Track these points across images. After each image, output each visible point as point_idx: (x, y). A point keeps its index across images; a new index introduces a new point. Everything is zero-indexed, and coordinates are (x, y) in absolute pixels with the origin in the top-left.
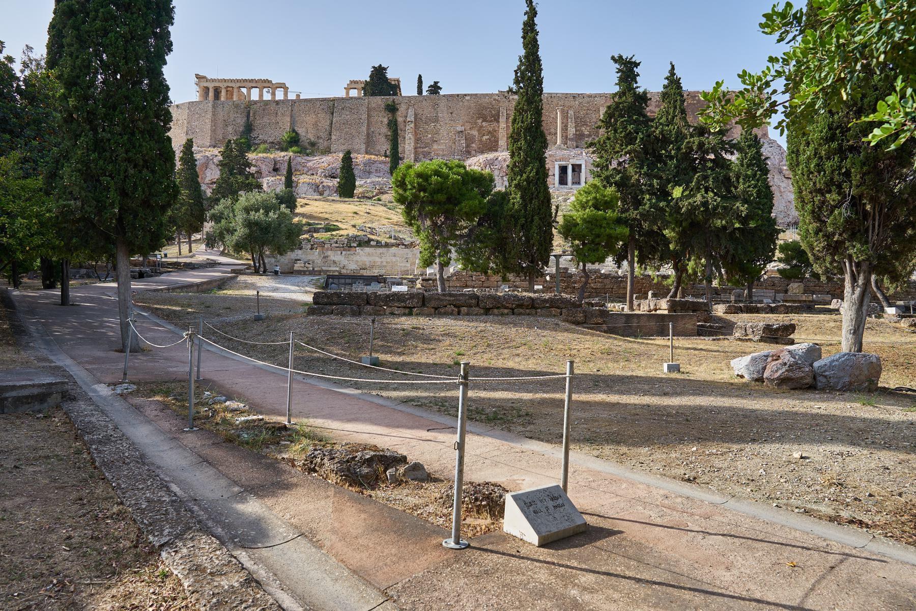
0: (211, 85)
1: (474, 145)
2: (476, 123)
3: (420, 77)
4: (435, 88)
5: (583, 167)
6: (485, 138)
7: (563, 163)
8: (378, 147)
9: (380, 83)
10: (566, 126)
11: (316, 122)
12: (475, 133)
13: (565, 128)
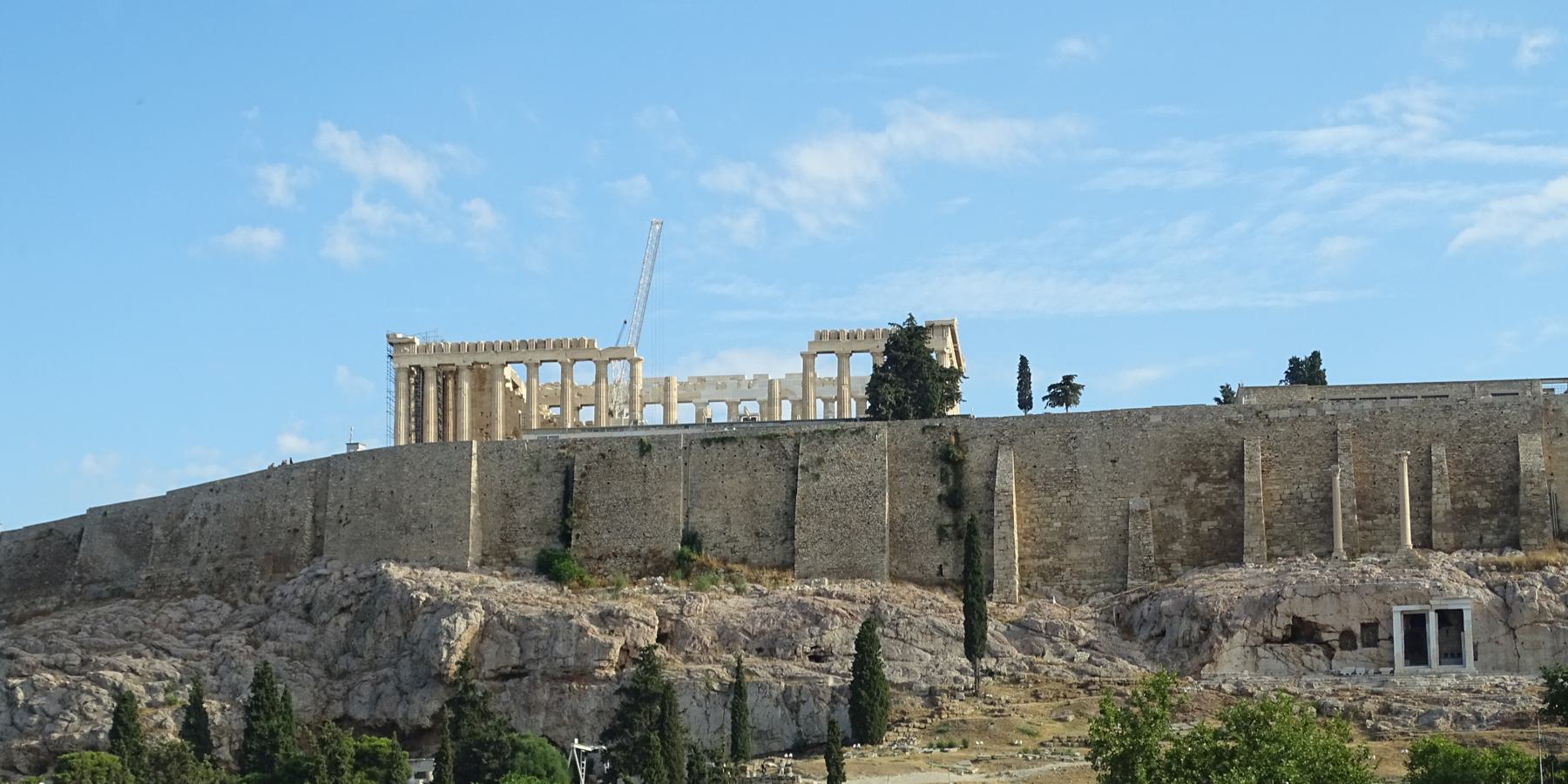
0: (428, 362)
1: (1177, 547)
2: (1178, 486)
3: (1024, 363)
4: (1065, 391)
5: (1467, 617)
6: (1206, 526)
7: (1414, 608)
8: (920, 558)
9: (910, 372)
10: (1427, 488)
11: (751, 494)
12: (1179, 513)
13: (1423, 495)
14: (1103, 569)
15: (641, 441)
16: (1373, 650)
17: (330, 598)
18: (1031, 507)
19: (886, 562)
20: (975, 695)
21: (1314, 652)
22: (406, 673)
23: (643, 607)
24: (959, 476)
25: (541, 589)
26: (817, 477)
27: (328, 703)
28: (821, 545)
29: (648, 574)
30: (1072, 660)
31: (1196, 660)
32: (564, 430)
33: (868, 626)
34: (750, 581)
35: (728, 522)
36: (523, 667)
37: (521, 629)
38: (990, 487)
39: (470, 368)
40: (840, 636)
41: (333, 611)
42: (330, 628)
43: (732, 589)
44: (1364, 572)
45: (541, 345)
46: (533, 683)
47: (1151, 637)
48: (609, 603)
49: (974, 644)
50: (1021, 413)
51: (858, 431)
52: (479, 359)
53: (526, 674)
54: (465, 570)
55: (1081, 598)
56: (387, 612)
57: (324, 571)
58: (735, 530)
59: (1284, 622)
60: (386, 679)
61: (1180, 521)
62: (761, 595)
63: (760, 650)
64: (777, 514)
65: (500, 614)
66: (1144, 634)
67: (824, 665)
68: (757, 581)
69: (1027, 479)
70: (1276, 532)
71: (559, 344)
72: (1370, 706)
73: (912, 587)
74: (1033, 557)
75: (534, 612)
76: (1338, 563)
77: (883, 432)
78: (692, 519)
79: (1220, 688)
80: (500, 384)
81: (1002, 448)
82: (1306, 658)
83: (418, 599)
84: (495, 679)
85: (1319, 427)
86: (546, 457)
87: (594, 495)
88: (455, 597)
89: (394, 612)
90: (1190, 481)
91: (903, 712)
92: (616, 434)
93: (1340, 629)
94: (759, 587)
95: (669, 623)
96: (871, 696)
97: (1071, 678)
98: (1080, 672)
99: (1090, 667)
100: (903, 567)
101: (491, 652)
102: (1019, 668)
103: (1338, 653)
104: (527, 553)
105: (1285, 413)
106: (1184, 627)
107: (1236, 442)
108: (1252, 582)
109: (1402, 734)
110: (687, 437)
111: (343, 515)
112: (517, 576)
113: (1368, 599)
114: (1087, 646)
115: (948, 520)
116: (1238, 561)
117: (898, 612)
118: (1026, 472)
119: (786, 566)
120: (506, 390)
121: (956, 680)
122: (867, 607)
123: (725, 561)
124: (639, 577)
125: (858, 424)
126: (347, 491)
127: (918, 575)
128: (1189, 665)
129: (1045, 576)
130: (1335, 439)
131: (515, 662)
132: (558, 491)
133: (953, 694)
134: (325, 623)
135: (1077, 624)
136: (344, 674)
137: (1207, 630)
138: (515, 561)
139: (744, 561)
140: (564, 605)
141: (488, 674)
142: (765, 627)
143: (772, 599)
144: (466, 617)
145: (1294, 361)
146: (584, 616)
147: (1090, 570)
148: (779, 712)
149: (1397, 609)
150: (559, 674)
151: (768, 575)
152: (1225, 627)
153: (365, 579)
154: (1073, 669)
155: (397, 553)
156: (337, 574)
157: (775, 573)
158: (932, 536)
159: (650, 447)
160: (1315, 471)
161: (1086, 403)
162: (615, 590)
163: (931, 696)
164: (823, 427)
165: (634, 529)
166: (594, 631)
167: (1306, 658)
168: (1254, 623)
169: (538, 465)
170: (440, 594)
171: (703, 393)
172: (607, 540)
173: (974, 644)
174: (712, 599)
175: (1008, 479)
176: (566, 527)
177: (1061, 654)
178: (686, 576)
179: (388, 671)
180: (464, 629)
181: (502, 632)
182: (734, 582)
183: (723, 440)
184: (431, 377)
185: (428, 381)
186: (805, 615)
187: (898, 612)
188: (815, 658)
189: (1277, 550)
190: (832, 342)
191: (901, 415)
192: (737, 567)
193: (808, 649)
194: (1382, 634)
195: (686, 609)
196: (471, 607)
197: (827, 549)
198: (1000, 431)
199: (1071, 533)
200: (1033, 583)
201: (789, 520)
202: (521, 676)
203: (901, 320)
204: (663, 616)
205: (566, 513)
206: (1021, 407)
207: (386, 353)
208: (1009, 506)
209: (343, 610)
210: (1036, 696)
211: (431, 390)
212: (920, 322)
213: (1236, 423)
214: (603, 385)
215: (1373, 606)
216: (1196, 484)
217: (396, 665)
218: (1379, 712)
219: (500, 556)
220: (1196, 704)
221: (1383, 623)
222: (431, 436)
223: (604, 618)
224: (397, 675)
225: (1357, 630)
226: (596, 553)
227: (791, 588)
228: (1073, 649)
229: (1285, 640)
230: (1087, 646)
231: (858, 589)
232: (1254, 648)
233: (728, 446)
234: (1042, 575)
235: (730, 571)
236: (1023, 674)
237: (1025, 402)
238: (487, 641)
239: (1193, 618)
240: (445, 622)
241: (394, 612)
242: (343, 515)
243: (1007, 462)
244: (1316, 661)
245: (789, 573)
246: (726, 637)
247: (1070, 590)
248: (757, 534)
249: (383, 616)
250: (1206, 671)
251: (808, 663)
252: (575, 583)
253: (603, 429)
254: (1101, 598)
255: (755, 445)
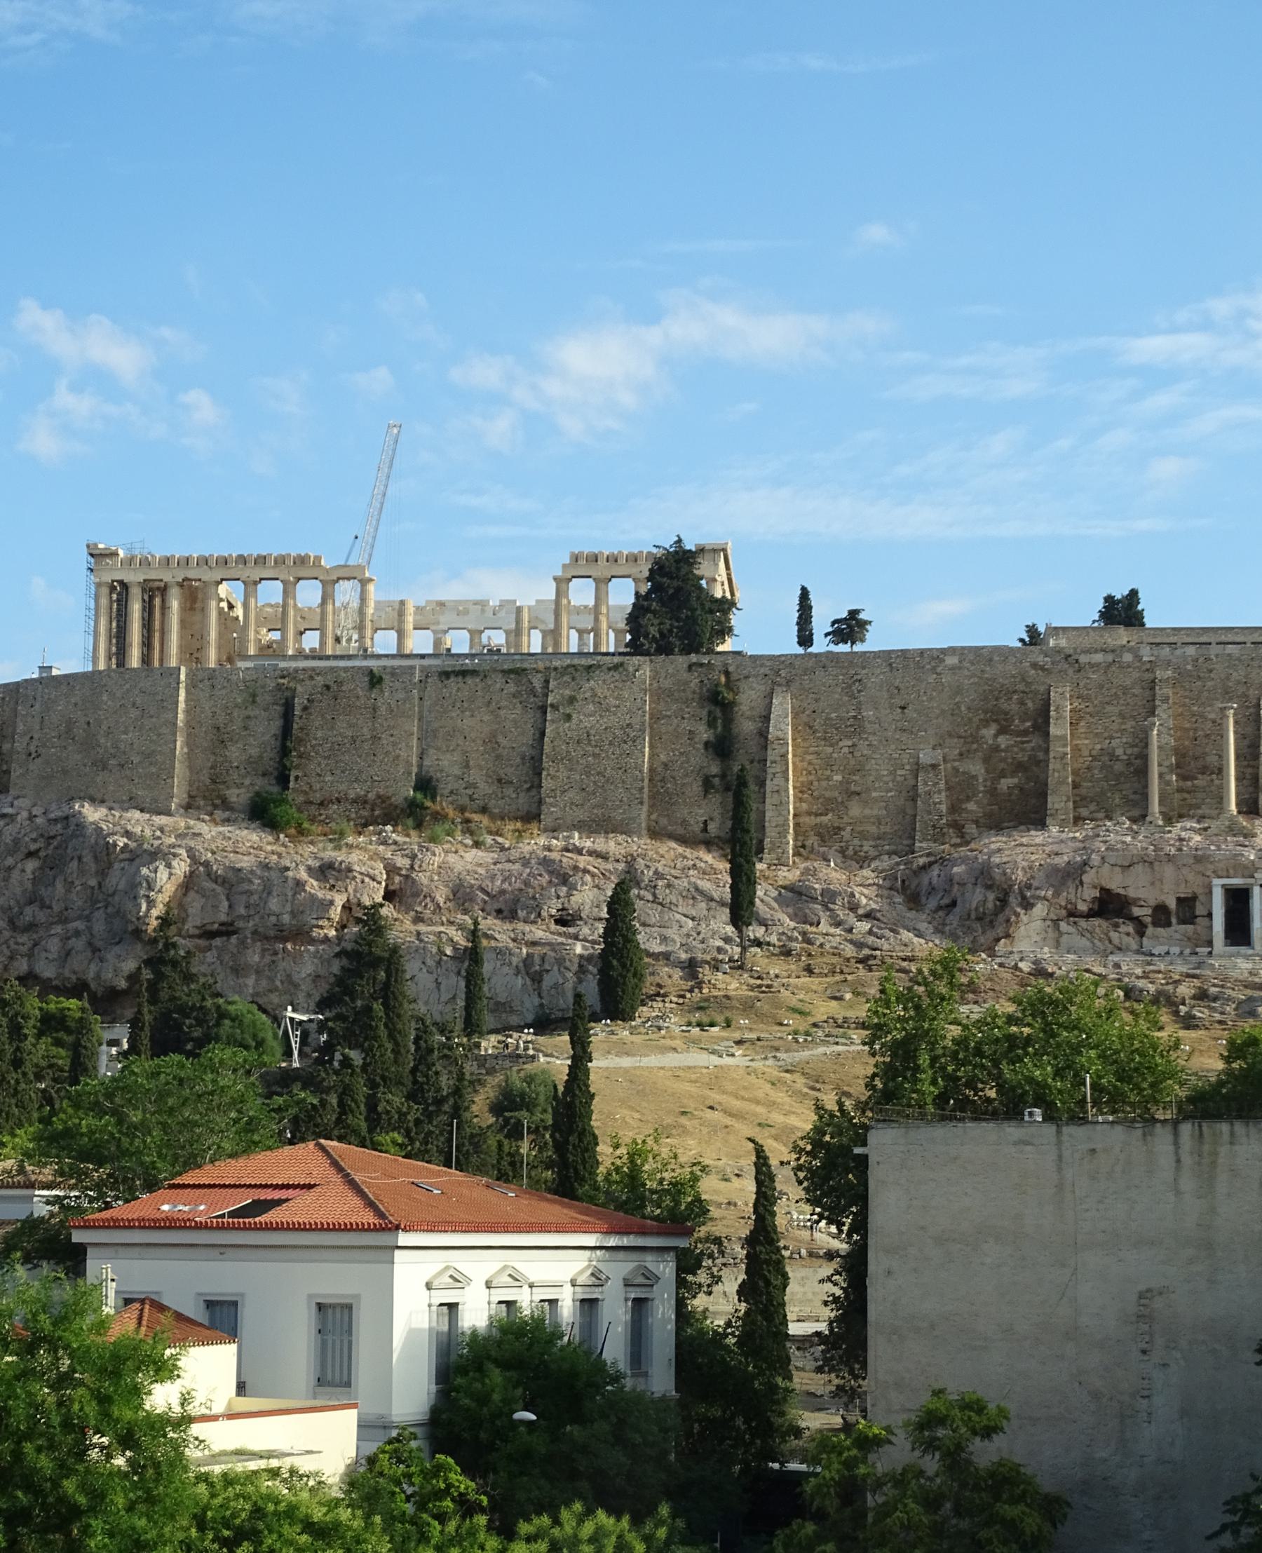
1: (971, 806)
2: (975, 738)
3: (805, 594)
6: (1005, 784)
7: (1237, 881)
8: (682, 812)
9: (677, 603)
11: (493, 735)
12: (976, 768)
14: (888, 829)
15: (371, 673)
16: (1190, 927)
17: (16, 841)
18: (809, 757)
19: (644, 816)
20: (741, 967)
21: (1123, 929)
22: (99, 927)
23: (368, 859)
24: (728, 721)
25: (255, 837)
26: (568, 717)
27: (11, 958)
28: (571, 794)
29: (375, 822)
30: (850, 930)
31: (991, 935)
32: (285, 657)
33: (621, 889)
34: (490, 833)
35: (467, 766)
36: (232, 924)
37: (231, 881)
38: (763, 734)
39: (181, 585)
40: (590, 898)
41: (20, 856)
42: (15, 874)
43: (469, 842)
44: (1181, 840)
45: (261, 560)
46: (242, 942)
47: (940, 908)
48: (330, 854)
49: (740, 909)
50: (800, 650)
51: (616, 667)
52: (191, 574)
53: (234, 933)
54: (168, 813)
55: (863, 861)
56: (80, 858)
57: (9, 810)
58: (475, 775)
59: (1090, 893)
60: (77, 933)
61: (975, 777)
62: (503, 849)
63: (499, 911)
64: (523, 758)
65: (207, 864)
66: (932, 903)
67: (571, 930)
68: (498, 833)
69: (805, 726)
70: (1083, 792)
71: (281, 561)
72: (1185, 990)
73: (673, 844)
74: (809, 813)
75: (246, 862)
76: (1152, 828)
77: (644, 669)
78: (427, 762)
79: (1016, 967)
80: (213, 604)
81: (778, 689)
82: (1114, 935)
83: (115, 845)
84: (199, 937)
85: (1136, 675)
86: (263, 687)
87: (314, 730)
88: (156, 843)
89: (88, 858)
90: (989, 732)
91: (659, 986)
92: (342, 664)
93: (1152, 903)
94: (500, 840)
95: (397, 879)
96: (624, 966)
97: (849, 951)
98: (859, 945)
99: (871, 940)
100: (664, 821)
101: (195, 905)
102: (791, 939)
103: (1150, 930)
104: (238, 796)
105: (1098, 658)
106: (977, 897)
107: (1042, 688)
108: (1055, 848)
109: (1220, 1022)
110: (423, 669)
111: (32, 749)
112: (227, 821)
113: (1185, 871)
114: (869, 916)
115: (715, 769)
116: (1041, 824)
117: (656, 872)
118: (804, 717)
119: (531, 817)
120: (220, 611)
121: (719, 950)
122: (621, 866)
123: (462, 810)
124: (366, 825)
125: (617, 659)
126: (38, 719)
127: (680, 831)
128: (982, 940)
129: (821, 838)
130: (1152, 689)
131: (223, 918)
132: (276, 725)
133: (716, 966)
134: (10, 869)
135: (857, 890)
136: (31, 927)
137: (1003, 902)
138: (225, 804)
139: (484, 810)
140: (280, 856)
141: (192, 931)
142: (506, 886)
143: (514, 854)
144: (169, 866)
145: (1109, 599)
146: (302, 868)
147: (873, 829)
148: (520, 981)
149: (1218, 883)
150: (272, 933)
151: (510, 826)
152: (1024, 897)
153: (56, 821)
154: (851, 942)
155: (91, 791)
156: (25, 814)
157: (519, 825)
158: (697, 787)
159: (380, 680)
160: (1129, 725)
161: (873, 642)
162: (337, 839)
163: (691, 968)
164: (576, 661)
165: (360, 772)
166: (313, 886)
167: (1114, 935)
168: (1057, 894)
169: (254, 696)
170: (140, 840)
171: (442, 619)
172: (332, 784)
173: (740, 909)
174: (447, 852)
175: (783, 725)
176: (284, 767)
177: (838, 924)
178: (419, 826)
179: (79, 925)
180: (166, 881)
181: (208, 885)
182: (472, 833)
183: (463, 673)
184: (136, 593)
185: (135, 598)
186: (551, 873)
187: (656, 872)
188: (561, 922)
189: (1084, 812)
190: (591, 565)
191: (664, 649)
192: (476, 817)
193: (553, 912)
194: (1200, 910)
195: (417, 863)
196: (175, 855)
197: (578, 799)
198: (776, 671)
199: (853, 788)
200: (809, 843)
201: (535, 766)
202: (229, 934)
203: (668, 542)
204: (391, 870)
205: (284, 752)
206: (800, 643)
207: (85, 566)
208: (784, 756)
209: (30, 855)
210: (809, 970)
211: (136, 608)
212: (689, 545)
213: (1042, 668)
214: (330, 608)
215: (1191, 877)
216: (996, 736)
217: (88, 919)
218: (1194, 997)
219: (208, 799)
220: (989, 984)
221: (1202, 898)
222: (134, 661)
223: (325, 871)
224: (90, 929)
225: (1172, 904)
226: (318, 797)
227: (536, 843)
228: (852, 919)
229: (1090, 915)
230: (869, 916)
231: (613, 845)
232: (1056, 922)
233: (469, 680)
234: (819, 834)
235: (468, 821)
236: (794, 945)
237: (805, 639)
238: (192, 894)
239: (989, 888)
240: (144, 871)
241: (88, 858)
242: (32, 749)
243: (783, 705)
244: (1126, 939)
245: (534, 825)
246: (461, 896)
247: (850, 852)
248: (500, 781)
249: (75, 864)
250: (1001, 947)
251: (553, 927)
252: (293, 831)
253: (328, 658)
254: (885, 863)
255: (499, 680)
